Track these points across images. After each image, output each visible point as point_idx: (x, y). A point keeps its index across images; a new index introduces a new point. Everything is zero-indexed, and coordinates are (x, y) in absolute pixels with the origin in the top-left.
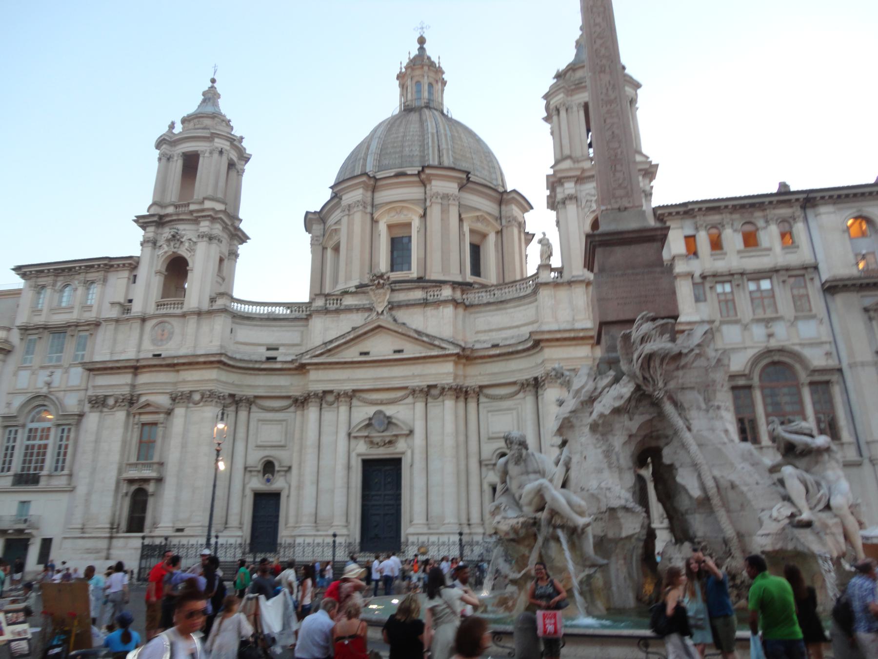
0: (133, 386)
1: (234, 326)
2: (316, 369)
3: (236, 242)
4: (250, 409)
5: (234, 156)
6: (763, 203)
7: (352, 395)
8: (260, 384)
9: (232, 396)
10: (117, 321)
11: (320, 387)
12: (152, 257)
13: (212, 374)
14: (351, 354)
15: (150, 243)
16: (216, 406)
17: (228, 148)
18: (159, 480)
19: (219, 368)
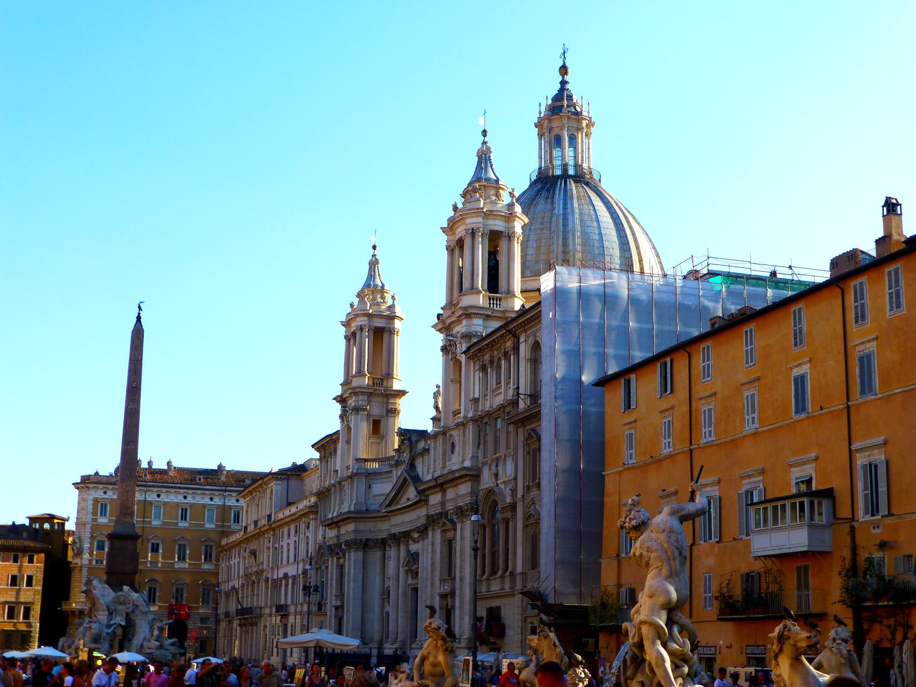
0: (338, 537)
1: (371, 481)
2: (393, 515)
3: (392, 401)
4: (384, 550)
5: (379, 323)
6: (494, 339)
7: (406, 535)
8: (385, 528)
9: (367, 540)
10: (334, 485)
11: (394, 531)
12: (343, 429)
13: (351, 527)
14: (403, 502)
15: (342, 417)
16: (356, 550)
17: (366, 323)
18: (342, 607)
19: (354, 521)
